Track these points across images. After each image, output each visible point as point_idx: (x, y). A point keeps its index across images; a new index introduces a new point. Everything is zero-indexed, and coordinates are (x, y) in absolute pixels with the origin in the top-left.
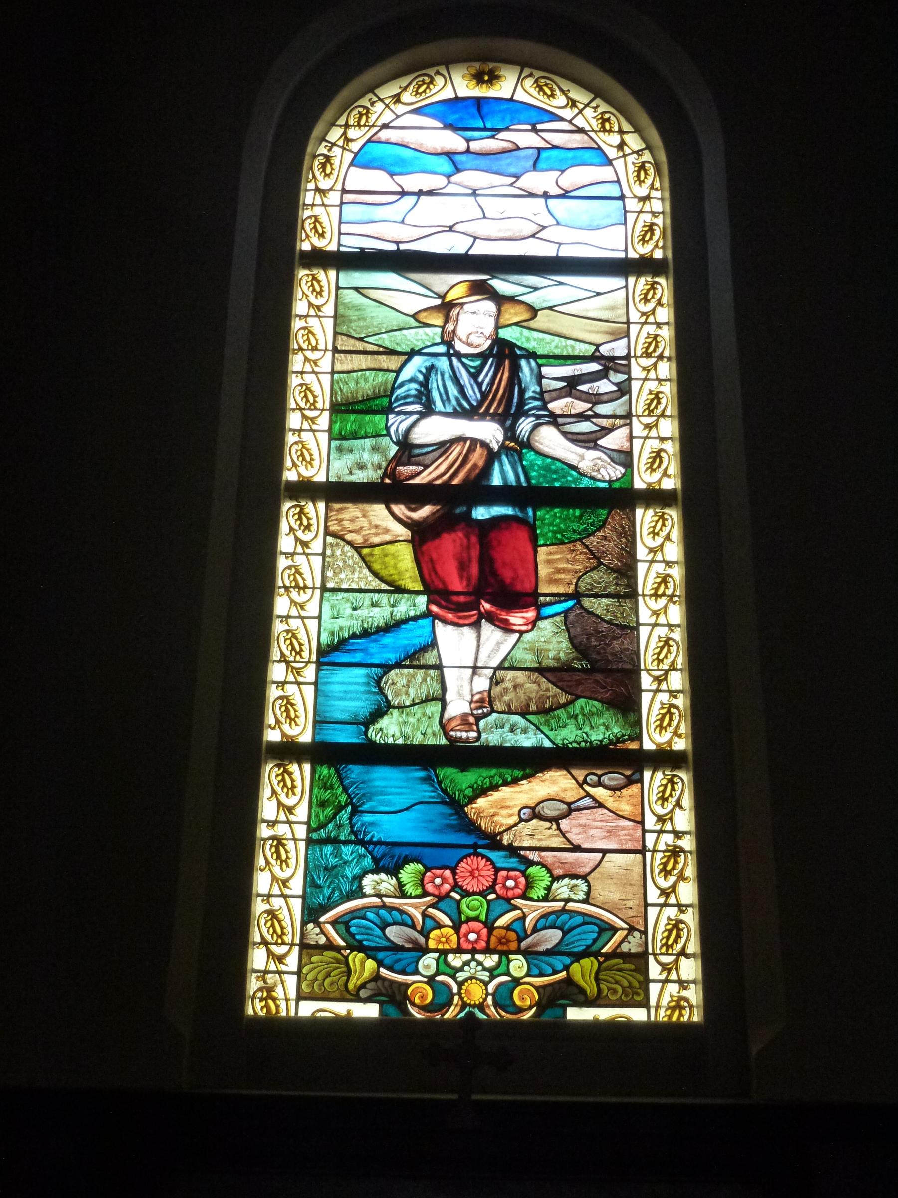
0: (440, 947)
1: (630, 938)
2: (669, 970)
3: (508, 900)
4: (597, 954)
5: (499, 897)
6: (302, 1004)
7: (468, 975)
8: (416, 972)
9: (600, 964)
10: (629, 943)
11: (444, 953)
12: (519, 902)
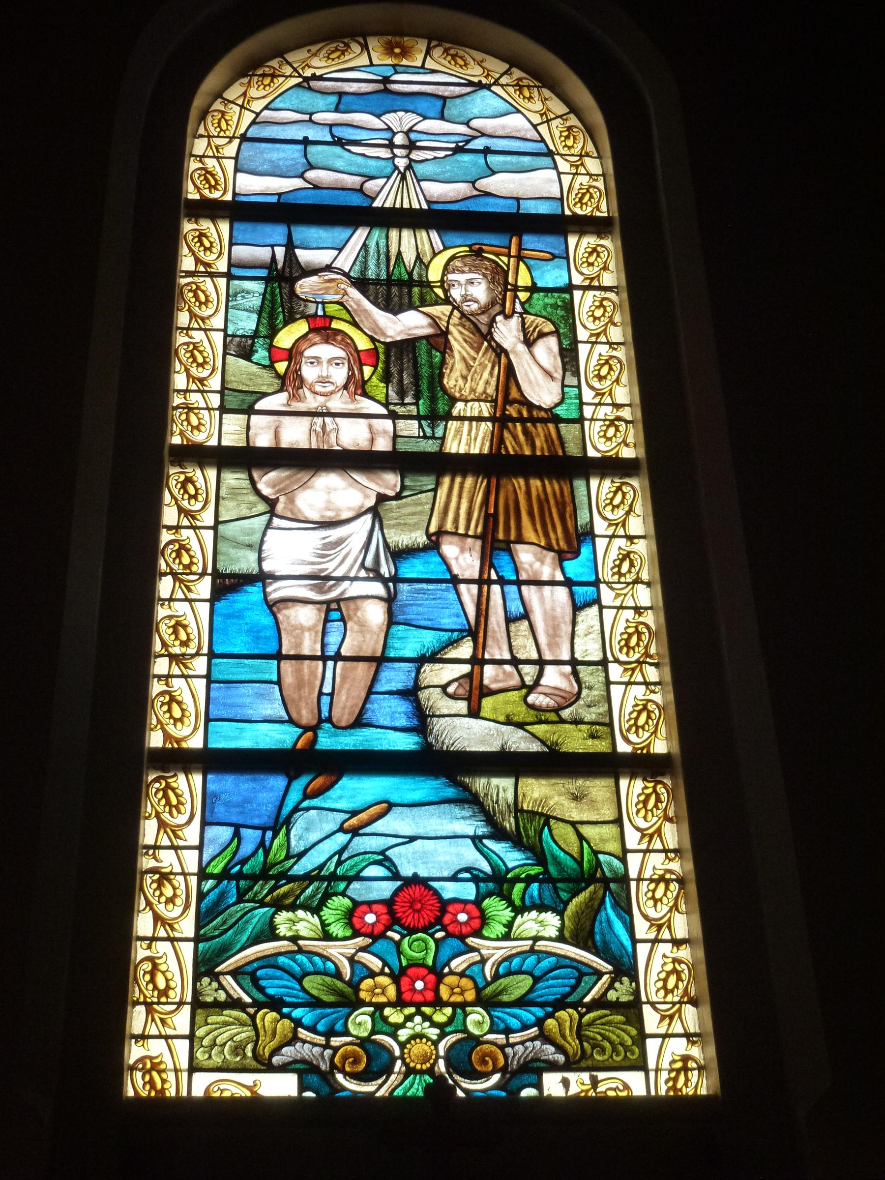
0: (374, 1000)
1: (617, 985)
2: (660, 927)
3: (462, 938)
4: (575, 1005)
5: (449, 935)
6: (196, 1076)
7: (411, 1032)
8: (347, 1033)
9: (582, 1016)
10: (616, 991)
11: (380, 1007)
12: (472, 941)
